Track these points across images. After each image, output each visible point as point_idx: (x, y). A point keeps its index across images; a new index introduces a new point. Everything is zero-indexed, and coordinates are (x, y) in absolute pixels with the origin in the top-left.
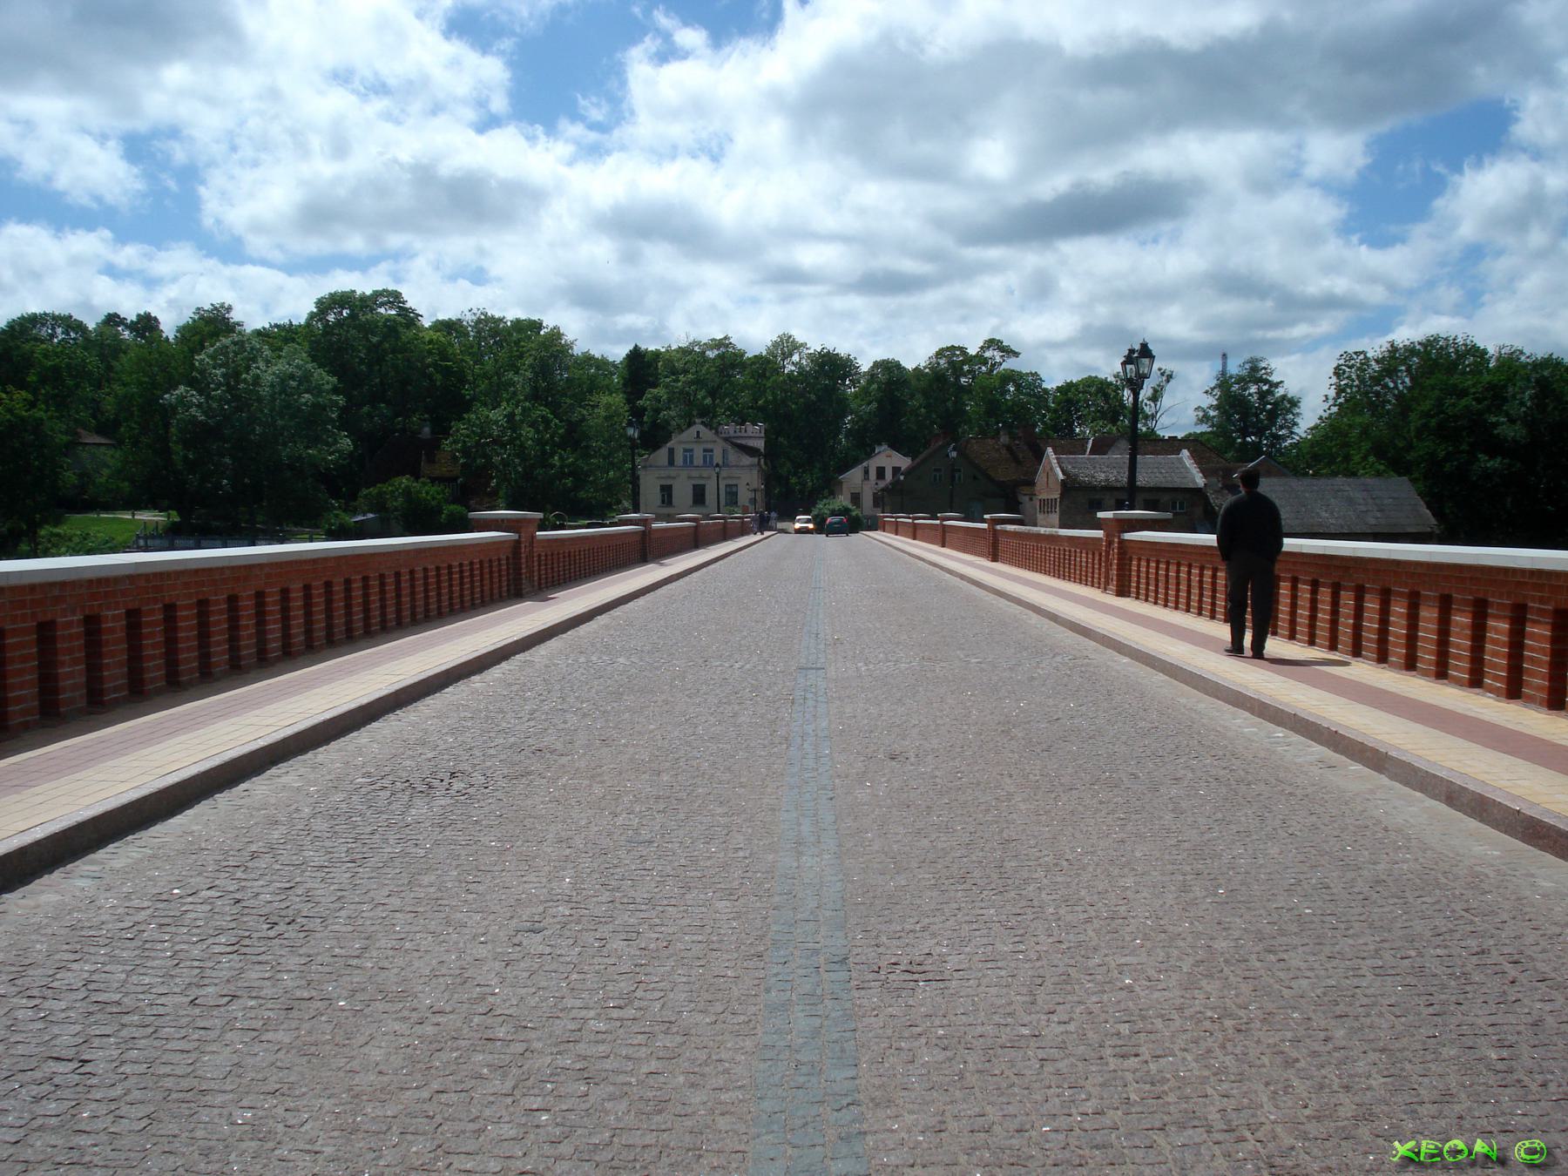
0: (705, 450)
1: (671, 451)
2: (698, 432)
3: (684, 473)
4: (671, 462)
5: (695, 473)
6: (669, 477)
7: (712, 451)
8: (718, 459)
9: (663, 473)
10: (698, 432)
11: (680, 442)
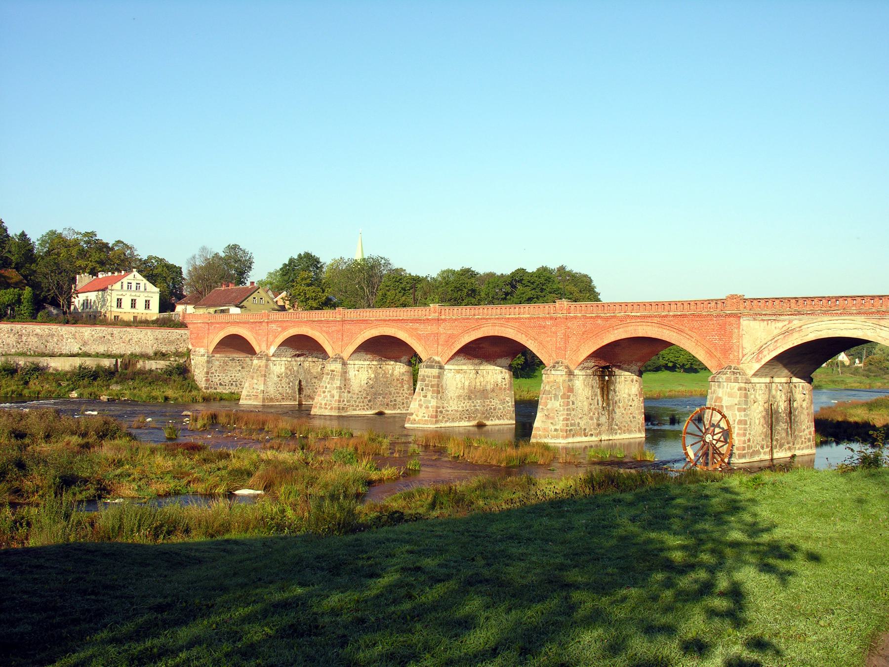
0: (137, 284)
1: (122, 283)
3: (128, 293)
4: (122, 288)
5: (133, 294)
6: (122, 295)
7: (139, 284)
8: (142, 289)
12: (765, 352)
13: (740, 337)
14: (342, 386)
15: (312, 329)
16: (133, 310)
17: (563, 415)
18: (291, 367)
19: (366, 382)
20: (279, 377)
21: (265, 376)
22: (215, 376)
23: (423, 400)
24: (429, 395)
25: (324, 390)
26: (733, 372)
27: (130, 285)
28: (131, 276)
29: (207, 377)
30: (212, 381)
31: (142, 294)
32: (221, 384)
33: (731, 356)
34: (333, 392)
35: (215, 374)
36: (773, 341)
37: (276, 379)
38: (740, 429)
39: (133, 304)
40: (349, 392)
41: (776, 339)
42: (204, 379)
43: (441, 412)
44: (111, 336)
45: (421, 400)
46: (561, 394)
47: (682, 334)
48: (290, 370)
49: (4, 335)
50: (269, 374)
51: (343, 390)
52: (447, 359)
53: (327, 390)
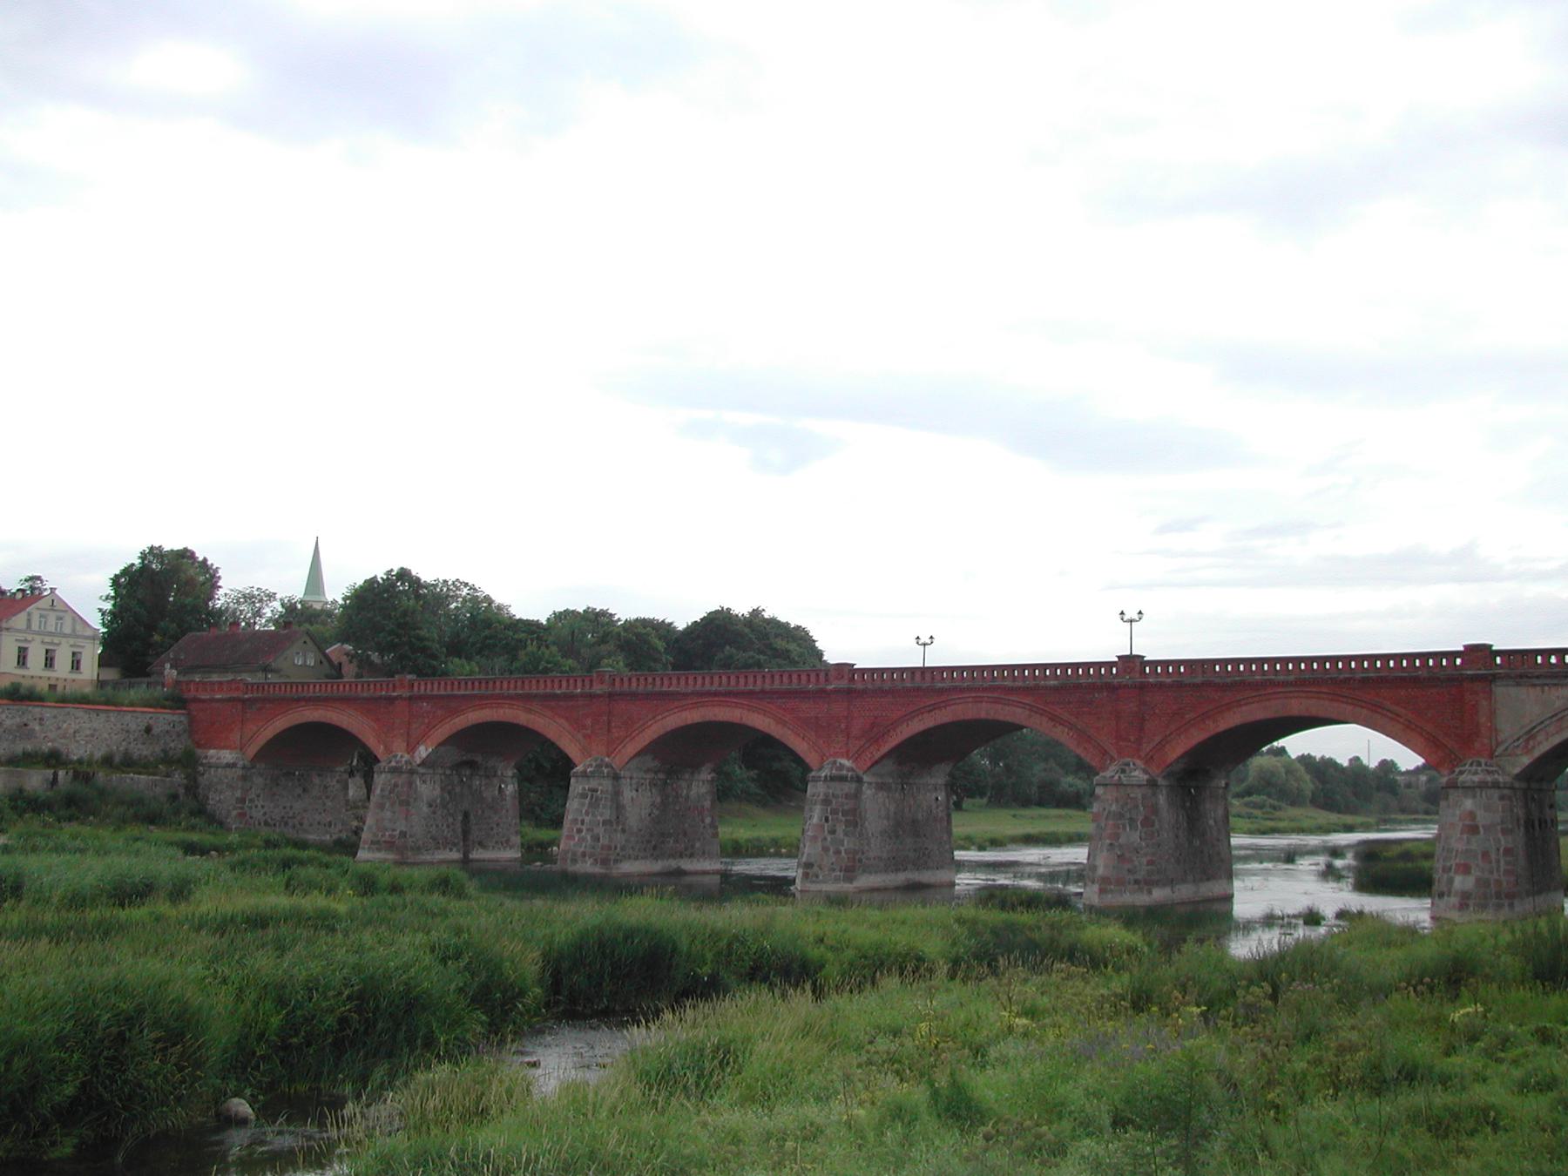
1: (29, 614)
3: (38, 638)
5: (47, 639)
6: (26, 640)
9: (21, 636)
11: (38, 609)
12: (1540, 737)
13: (1492, 714)
14: (614, 818)
15: (529, 711)
17: (1146, 855)
18: (450, 787)
19: (648, 811)
20: (431, 806)
21: (408, 804)
22: (256, 807)
23: (829, 839)
24: (840, 829)
25: (579, 826)
26: (1487, 771)
27: (43, 620)
29: (242, 808)
30: (251, 818)
32: (266, 823)
33: (1477, 745)
34: (596, 831)
35: (256, 802)
36: (1555, 719)
37: (425, 809)
38: (1507, 863)
39: (49, 662)
40: (623, 831)
41: (1560, 716)
42: (234, 813)
43: (860, 861)
44: (41, 724)
45: (825, 839)
46: (1141, 818)
47: (1380, 710)
48: (449, 793)
50: (415, 799)
51: (615, 826)
52: (869, 764)
53: (584, 828)
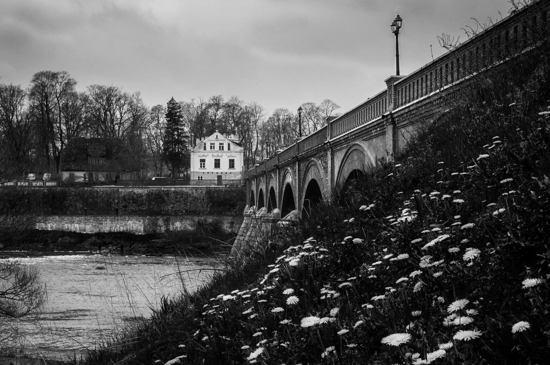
0: (220, 144)
2: (217, 136)
3: (211, 154)
4: (205, 149)
5: (216, 154)
7: (223, 144)
8: (226, 148)
9: (201, 154)
10: (217, 136)
16: (217, 170)
28: (213, 137)
31: (224, 154)
39: (217, 164)
49: (73, 198)
